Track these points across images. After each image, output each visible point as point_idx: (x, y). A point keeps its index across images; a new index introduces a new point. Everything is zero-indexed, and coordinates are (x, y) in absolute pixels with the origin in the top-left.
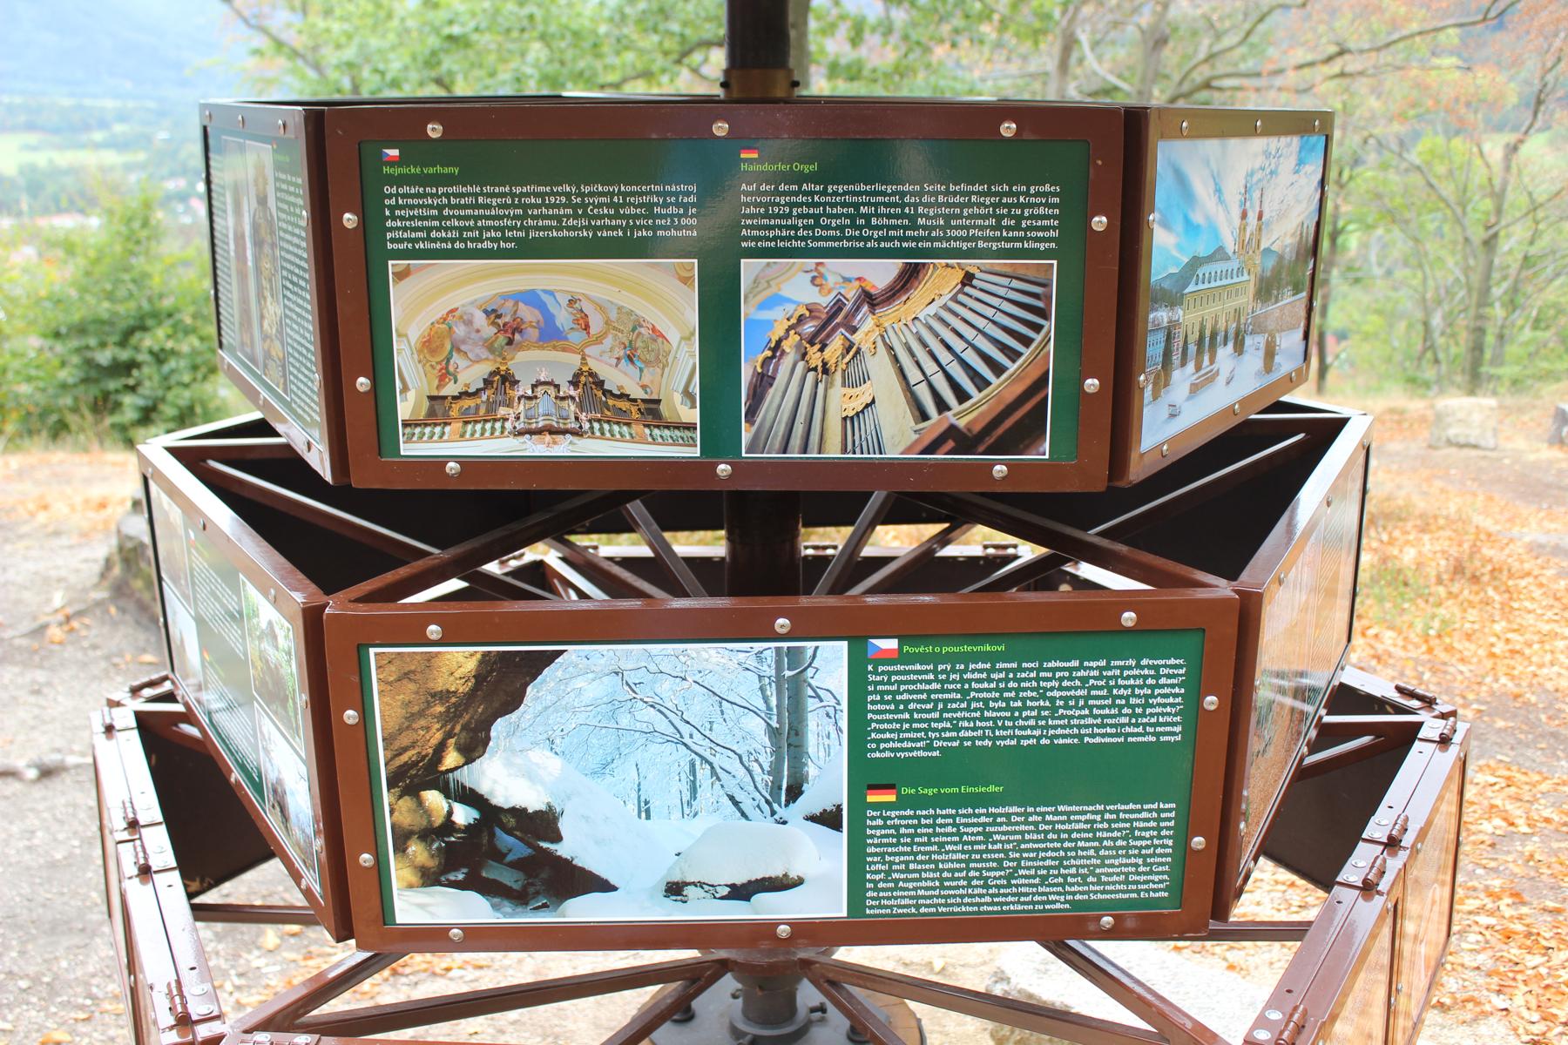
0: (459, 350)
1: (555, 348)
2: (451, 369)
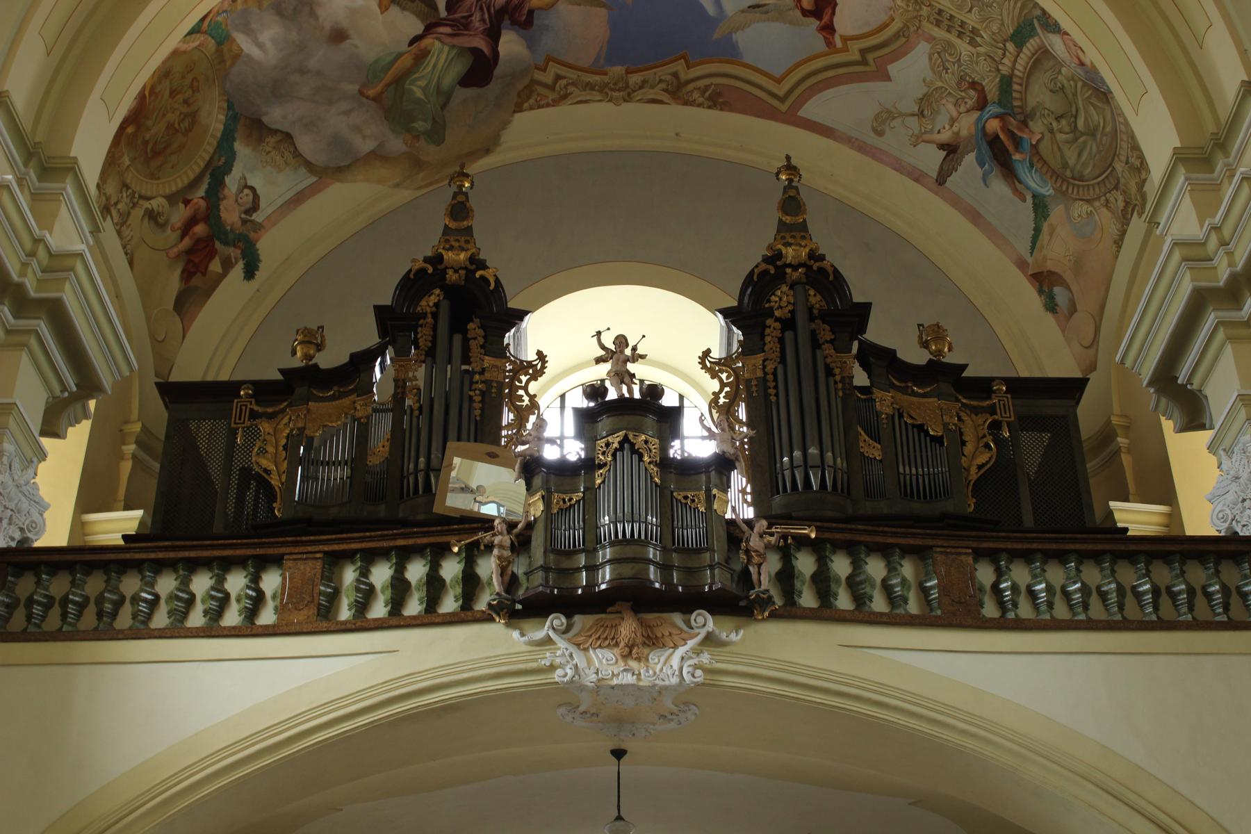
0: (258, 130)
1: (677, 92)
2: (230, 215)
